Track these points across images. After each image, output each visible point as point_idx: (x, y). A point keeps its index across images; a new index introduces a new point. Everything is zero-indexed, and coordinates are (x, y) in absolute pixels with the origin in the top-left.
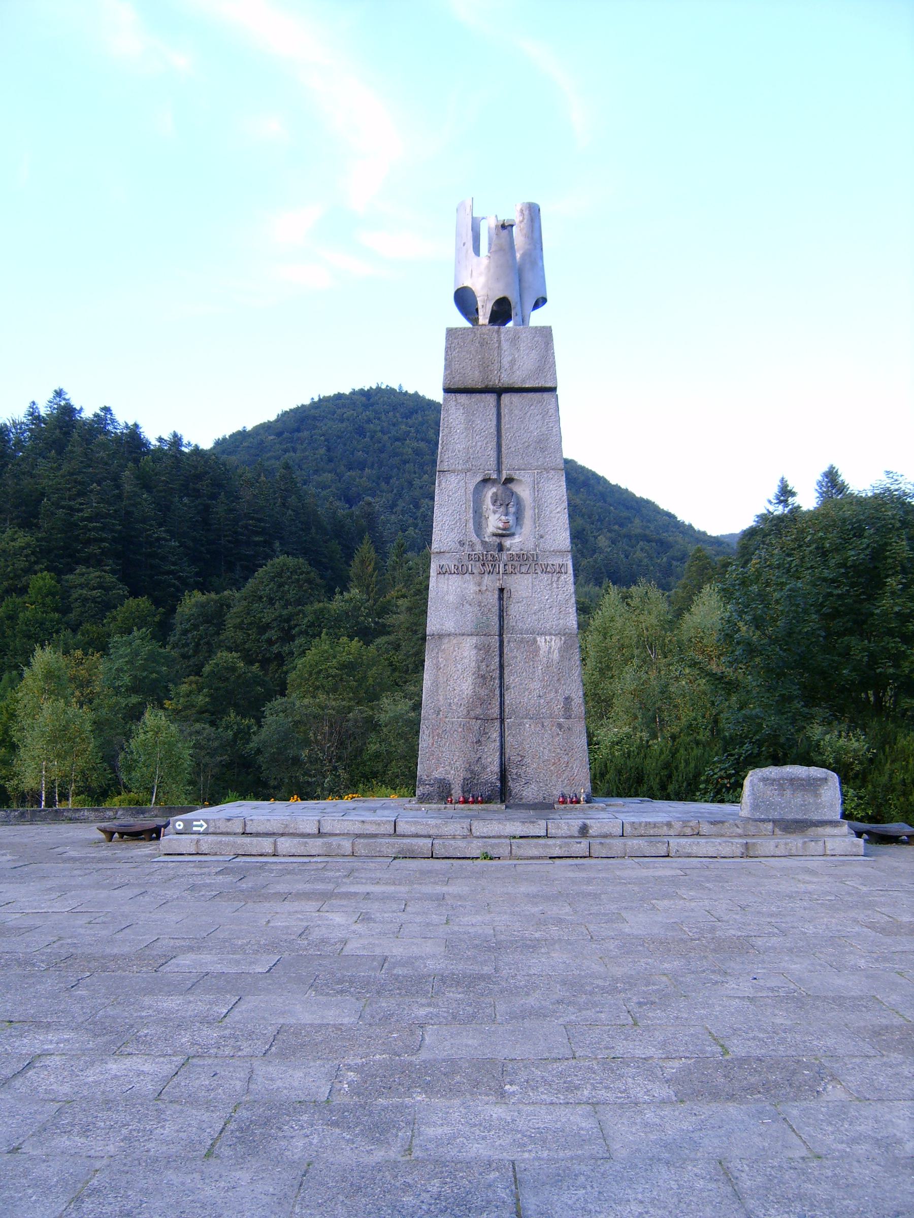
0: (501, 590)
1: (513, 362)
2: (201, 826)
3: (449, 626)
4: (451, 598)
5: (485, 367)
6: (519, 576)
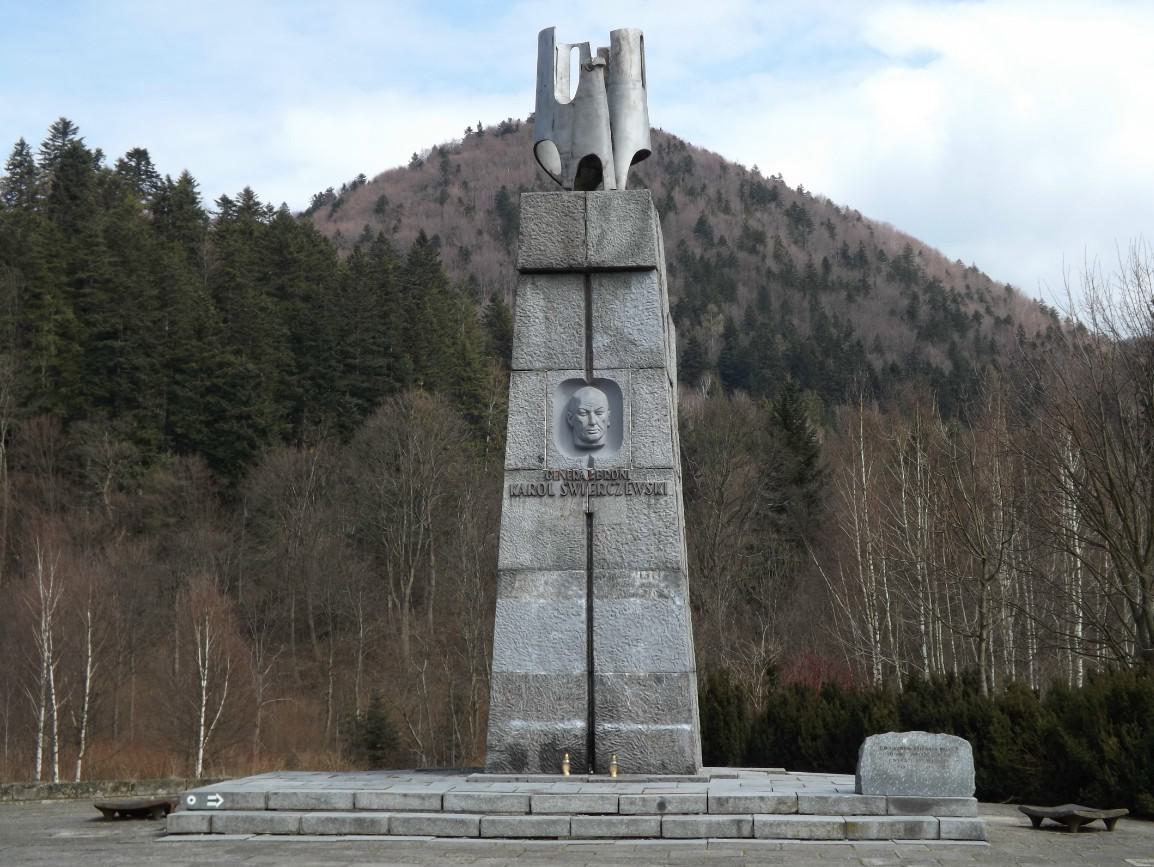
0: (590, 516)
1: (602, 236)
2: (217, 800)
3: (525, 558)
4: (527, 525)
5: (568, 243)
6: (607, 498)
